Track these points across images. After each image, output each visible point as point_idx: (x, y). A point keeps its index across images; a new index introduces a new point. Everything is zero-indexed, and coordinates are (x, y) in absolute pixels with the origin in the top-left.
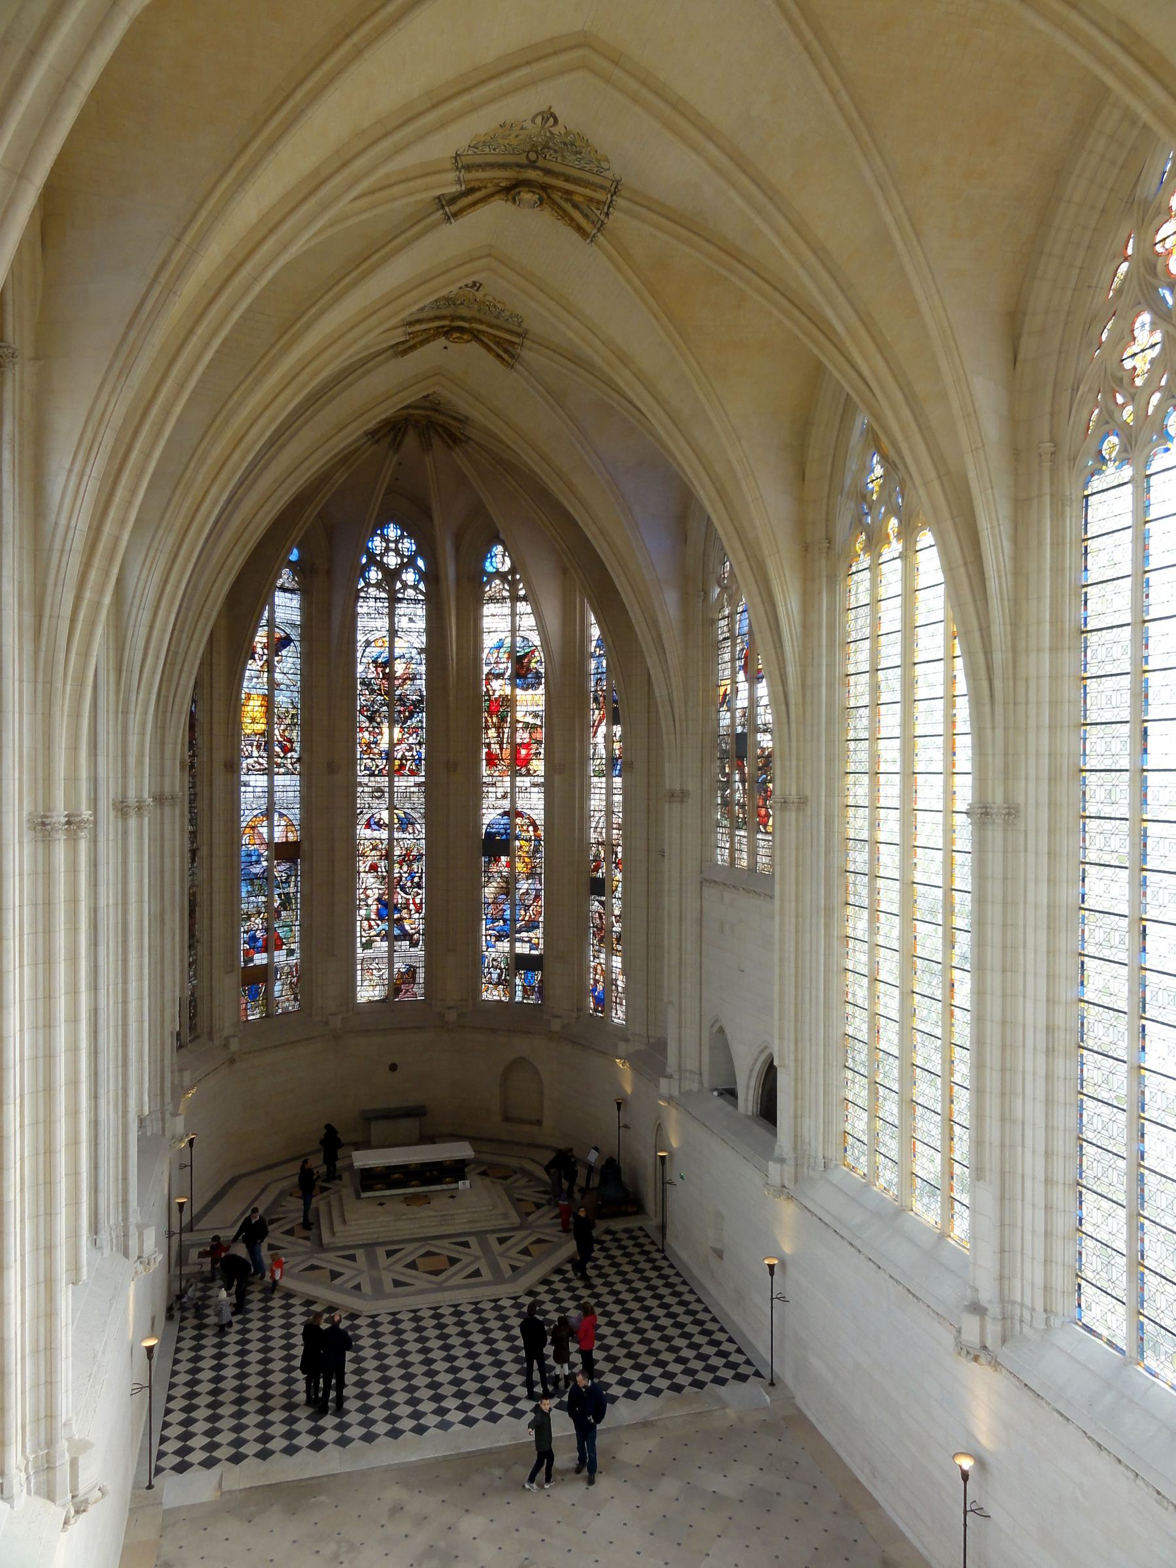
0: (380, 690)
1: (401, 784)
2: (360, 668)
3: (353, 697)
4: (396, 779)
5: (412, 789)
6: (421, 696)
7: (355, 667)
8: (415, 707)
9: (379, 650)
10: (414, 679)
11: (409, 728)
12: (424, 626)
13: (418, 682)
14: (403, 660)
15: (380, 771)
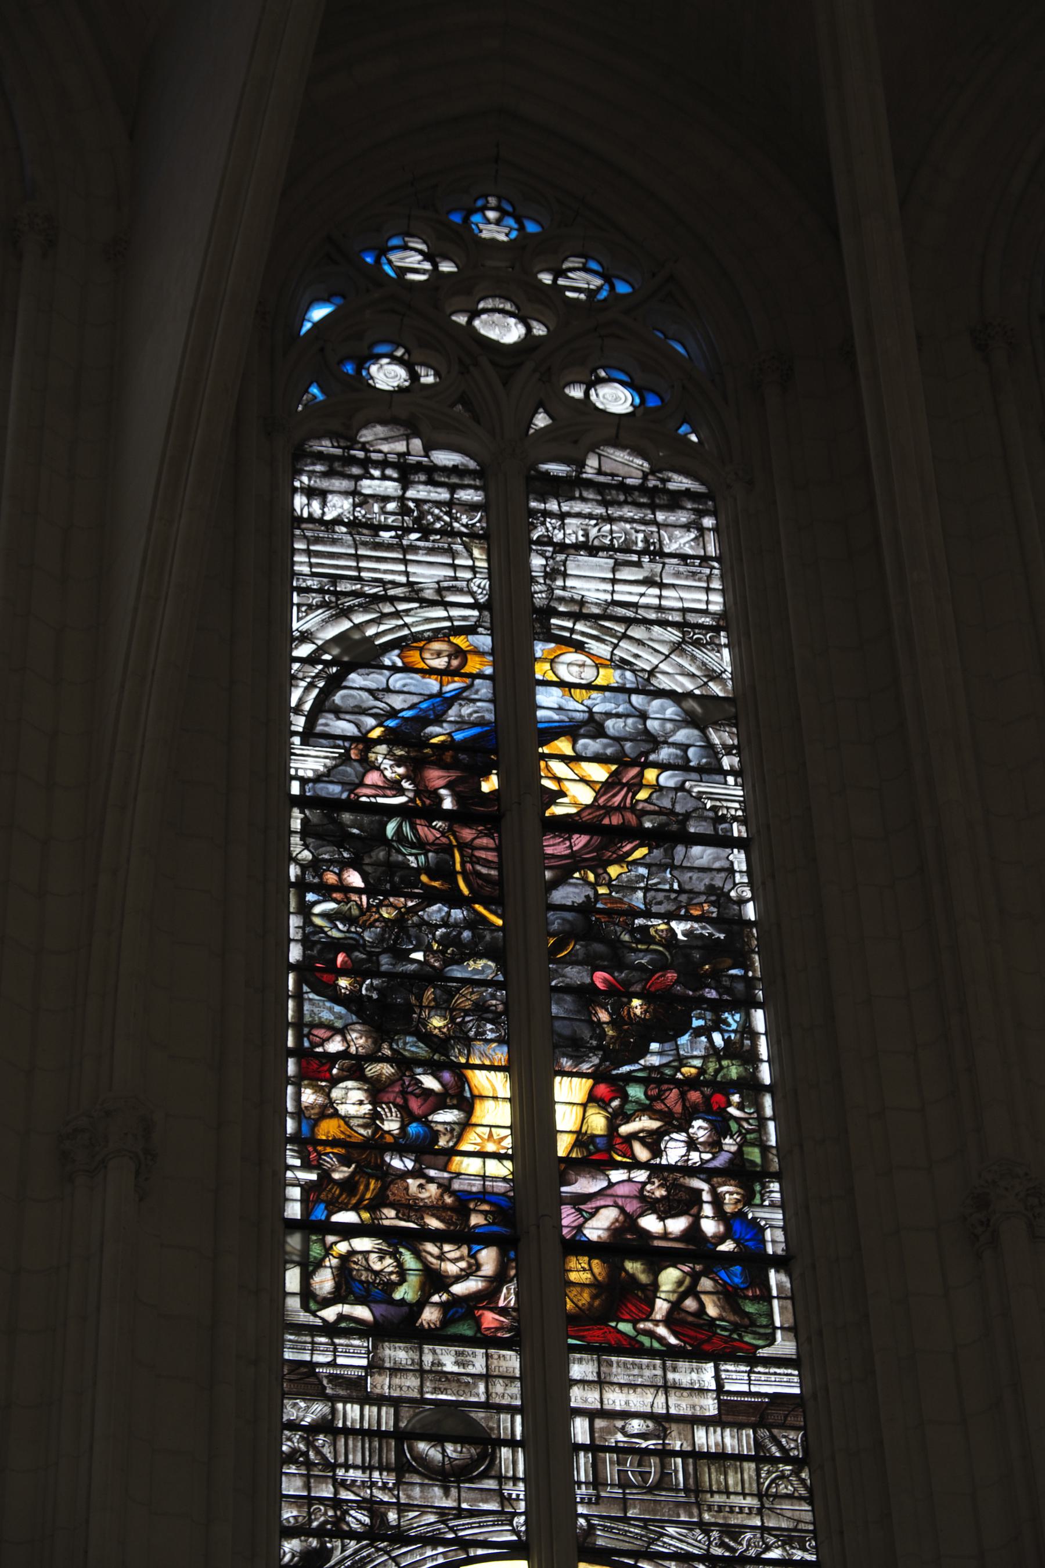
0: (443, 871)
1: (616, 1400)
2: (309, 762)
3: (270, 894)
4: (581, 1369)
5: (704, 1439)
6: (729, 919)
7: (287, 753)
8: (694, 978)
9: (432, 684)
10: (670, 834)
11: (653, 1079)
12: (717, 603)
13: (701, 855)
14: (590, 745)
15: (463, 1309)
